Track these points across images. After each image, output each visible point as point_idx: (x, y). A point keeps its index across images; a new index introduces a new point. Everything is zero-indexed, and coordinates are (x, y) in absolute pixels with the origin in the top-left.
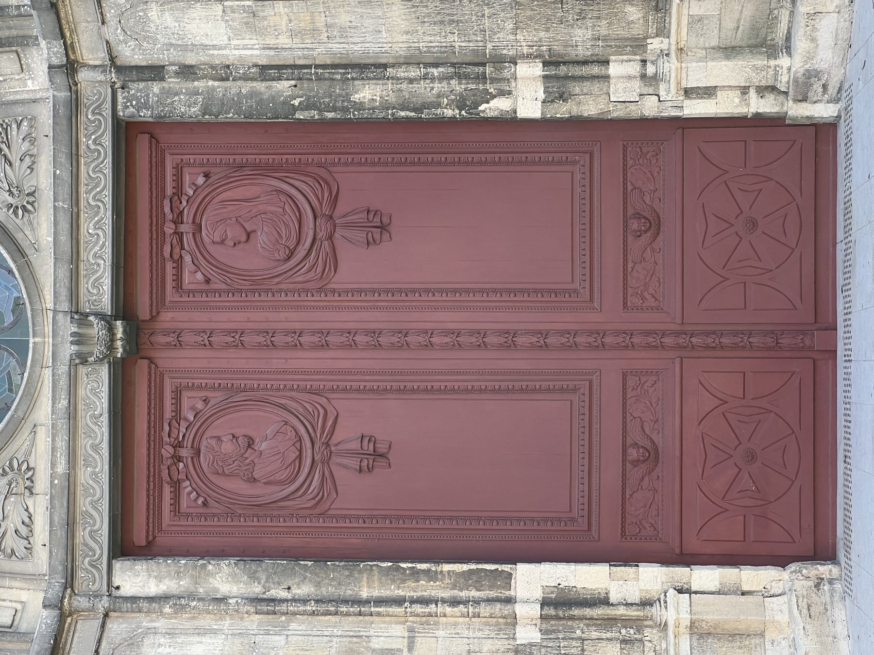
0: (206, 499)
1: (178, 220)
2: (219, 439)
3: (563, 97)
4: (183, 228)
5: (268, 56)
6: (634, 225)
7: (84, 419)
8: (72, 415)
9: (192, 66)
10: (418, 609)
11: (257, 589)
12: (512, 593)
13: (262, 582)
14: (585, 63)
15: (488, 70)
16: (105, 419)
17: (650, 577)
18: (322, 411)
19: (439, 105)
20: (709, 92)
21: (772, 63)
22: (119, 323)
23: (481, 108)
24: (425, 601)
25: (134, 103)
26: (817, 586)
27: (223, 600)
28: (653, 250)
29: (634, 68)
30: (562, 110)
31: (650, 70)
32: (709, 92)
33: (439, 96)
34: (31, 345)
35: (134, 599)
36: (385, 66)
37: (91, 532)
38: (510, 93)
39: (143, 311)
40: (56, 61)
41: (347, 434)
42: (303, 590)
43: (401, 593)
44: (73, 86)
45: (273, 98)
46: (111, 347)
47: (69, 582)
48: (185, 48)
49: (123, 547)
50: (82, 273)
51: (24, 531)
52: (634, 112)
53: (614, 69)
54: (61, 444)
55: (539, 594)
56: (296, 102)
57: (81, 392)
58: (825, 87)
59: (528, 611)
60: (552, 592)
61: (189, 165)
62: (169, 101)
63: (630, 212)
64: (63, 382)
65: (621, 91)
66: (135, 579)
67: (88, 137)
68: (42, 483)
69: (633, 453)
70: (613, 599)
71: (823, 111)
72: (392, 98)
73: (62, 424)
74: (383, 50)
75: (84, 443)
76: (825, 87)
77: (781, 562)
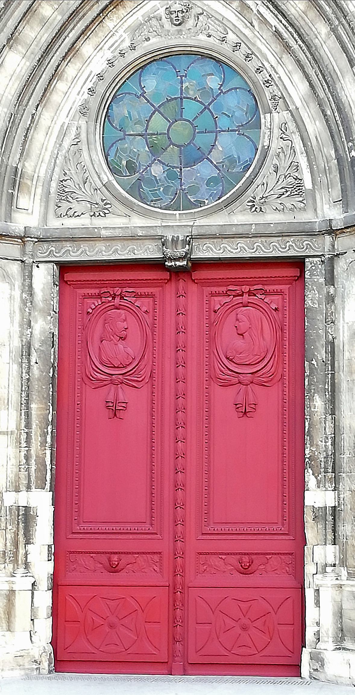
0: (91, 313)
1: (250, 293)
2: (125, 320)
3: (315, 518)
4: (246, 296)
5: (339, 346)
6: (246, 559)
7: (132, 245)
8: (133, 238)
9: (333, 301)
10: (24, 436)
11: (36, 344)
12: (33, 489)
13: (40, 348)
14: (334, 531)
15: (330, 475)
16: (132, 256)
17: (43, 568)
18: (140, 379)
19: (311, 446)
20: (317, 603)
21: (331, 640)
22: (185, 263)
23: (310, 470)
24: (28, 440)
25: (314, 268)
26: (36, 661)
27: (30, 325)
28: (231, 570)
29: (331, 560)
30: (308, 517)
31: (329, 569)
32: (317, 603)
33: (317, 445)
34: (175, 212)
35: (31, 276)
36: (333, 414)
37: (69, 250)
38: (319, 487)
39: (196, 275)
40: (334, 224)
41: (125, 394)
42: (36, 371)
43: (34, 426)
44: (321, 233)
45: (316, 348)
46: (170, 259)
47: (40, 240)
48: (343, 297)
49: (65, 268)
50: (215, 240)
51: (71, 213)
52: (308, 559)
53: (331, 549)
54: (117, 233)
55: (32, 505)
56: (314, 362)
57: (147, 242)
58: (316, 670)
59: (22, 499)
60: (33, 512)
61: (283, 299)
62: (315, 288)
63: (254, 557)
64: (152, 232)
65: (320, 552)
66: (43, 277)
67: (294, 242)
68: (99, 222)
69: (115, 558)
70: (29, 547)
71: (305, 670)
72: (316, 418)
73: (129, 233)
74: (342, 413)
75: (118, 245)
76: (316, 670)
77: (54, 642)
